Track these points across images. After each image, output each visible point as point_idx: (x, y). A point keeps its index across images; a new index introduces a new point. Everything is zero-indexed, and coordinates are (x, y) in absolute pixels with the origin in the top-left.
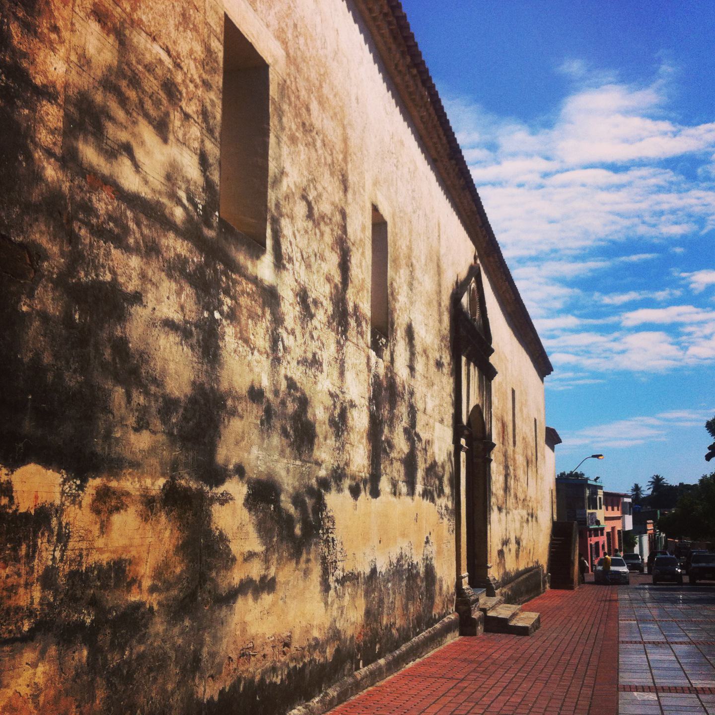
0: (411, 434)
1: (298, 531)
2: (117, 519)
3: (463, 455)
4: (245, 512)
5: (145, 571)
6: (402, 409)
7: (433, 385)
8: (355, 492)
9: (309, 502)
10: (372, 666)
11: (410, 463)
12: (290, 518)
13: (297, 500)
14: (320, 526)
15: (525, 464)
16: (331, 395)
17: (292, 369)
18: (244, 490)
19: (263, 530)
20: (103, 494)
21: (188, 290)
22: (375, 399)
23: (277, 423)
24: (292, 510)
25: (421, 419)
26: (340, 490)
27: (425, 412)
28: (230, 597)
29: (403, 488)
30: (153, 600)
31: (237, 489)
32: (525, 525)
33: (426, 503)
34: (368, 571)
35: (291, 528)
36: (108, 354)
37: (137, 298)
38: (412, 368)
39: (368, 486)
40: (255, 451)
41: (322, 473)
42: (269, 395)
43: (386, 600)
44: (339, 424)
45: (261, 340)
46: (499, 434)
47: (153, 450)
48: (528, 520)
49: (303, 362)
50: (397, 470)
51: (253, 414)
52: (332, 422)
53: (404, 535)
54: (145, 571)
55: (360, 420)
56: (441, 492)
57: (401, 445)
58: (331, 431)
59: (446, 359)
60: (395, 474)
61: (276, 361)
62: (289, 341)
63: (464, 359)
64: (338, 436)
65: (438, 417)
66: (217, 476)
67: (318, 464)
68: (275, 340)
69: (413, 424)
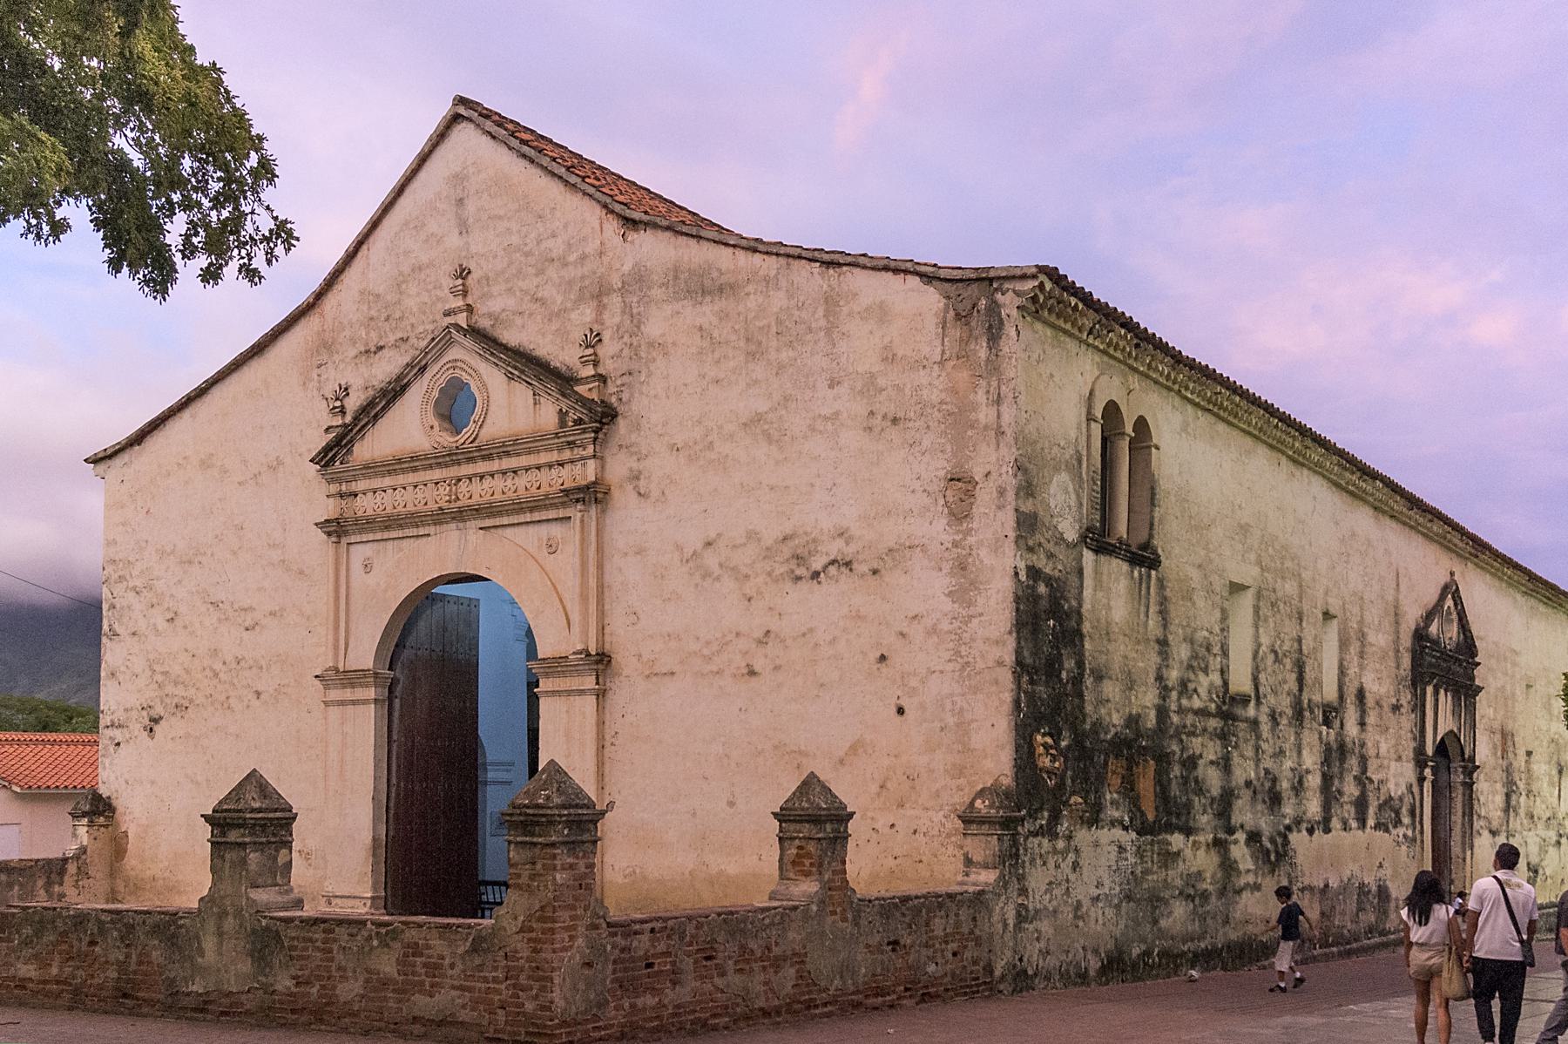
0: (1362, 780)
1: (1273, 858)
2: (1198, 853)
3: (1427, 786)
4: (1245, 850)
5: (1208, 875)
6: (1353, 762)
7: (1387, 729)
8: (1311, 831)
9: (1279, 840)
10: (1327, 950)
11: (1361, 805)
12: (1268, 851)
13: (1272, 840)
14: (1286, 854)
15: (1555, 772)
16: (1292, 770)
17: (1268, 763)
18: (1245, 836)
20: (1195, 842)
21: (1218, 742)
22: (1326, 761)
23: (1259, 797)
24: (1269, 845)
25: (1372, 765)
26: (1299, 831)
27: (1377, 756)
28: (1239, 892)
29: (1354, 824)
30: (1210, 888)
31: (1241, 836)
32: (1552, 850)
33: (1379, 834)
34: (1322, 885)
35: (1269, 857)
37: (1201, 756)
38: (1362, 724)
39: (1321, 826)
41: (1287, 821)
42: (1255, 782)
43: (1337, 907)
44: (1298, 787)
45: (1249, 752)
46: (1495, 747)
47: (1209, 822)
48: (1559, 843)
49: (1275, 755)
50: (1349, 811)
51: (1246, 794)
52: (1294, 788)
53: (1354, 860)
54: (1208, 875)
55: (1314, 781)
56: (1398, 822)
57: (1351, 789)
58: (1292, 794)
59: (1406, 698)
60: (1346, 815)
61: (1258, 761)
62: (1264, 746)
63: (1430, 689)
64: (1297, 795)
65: (1394, 756)
66: (1231, 831)
67: (1284, 817)
68: (1257, 748)
69: (1364, 770)
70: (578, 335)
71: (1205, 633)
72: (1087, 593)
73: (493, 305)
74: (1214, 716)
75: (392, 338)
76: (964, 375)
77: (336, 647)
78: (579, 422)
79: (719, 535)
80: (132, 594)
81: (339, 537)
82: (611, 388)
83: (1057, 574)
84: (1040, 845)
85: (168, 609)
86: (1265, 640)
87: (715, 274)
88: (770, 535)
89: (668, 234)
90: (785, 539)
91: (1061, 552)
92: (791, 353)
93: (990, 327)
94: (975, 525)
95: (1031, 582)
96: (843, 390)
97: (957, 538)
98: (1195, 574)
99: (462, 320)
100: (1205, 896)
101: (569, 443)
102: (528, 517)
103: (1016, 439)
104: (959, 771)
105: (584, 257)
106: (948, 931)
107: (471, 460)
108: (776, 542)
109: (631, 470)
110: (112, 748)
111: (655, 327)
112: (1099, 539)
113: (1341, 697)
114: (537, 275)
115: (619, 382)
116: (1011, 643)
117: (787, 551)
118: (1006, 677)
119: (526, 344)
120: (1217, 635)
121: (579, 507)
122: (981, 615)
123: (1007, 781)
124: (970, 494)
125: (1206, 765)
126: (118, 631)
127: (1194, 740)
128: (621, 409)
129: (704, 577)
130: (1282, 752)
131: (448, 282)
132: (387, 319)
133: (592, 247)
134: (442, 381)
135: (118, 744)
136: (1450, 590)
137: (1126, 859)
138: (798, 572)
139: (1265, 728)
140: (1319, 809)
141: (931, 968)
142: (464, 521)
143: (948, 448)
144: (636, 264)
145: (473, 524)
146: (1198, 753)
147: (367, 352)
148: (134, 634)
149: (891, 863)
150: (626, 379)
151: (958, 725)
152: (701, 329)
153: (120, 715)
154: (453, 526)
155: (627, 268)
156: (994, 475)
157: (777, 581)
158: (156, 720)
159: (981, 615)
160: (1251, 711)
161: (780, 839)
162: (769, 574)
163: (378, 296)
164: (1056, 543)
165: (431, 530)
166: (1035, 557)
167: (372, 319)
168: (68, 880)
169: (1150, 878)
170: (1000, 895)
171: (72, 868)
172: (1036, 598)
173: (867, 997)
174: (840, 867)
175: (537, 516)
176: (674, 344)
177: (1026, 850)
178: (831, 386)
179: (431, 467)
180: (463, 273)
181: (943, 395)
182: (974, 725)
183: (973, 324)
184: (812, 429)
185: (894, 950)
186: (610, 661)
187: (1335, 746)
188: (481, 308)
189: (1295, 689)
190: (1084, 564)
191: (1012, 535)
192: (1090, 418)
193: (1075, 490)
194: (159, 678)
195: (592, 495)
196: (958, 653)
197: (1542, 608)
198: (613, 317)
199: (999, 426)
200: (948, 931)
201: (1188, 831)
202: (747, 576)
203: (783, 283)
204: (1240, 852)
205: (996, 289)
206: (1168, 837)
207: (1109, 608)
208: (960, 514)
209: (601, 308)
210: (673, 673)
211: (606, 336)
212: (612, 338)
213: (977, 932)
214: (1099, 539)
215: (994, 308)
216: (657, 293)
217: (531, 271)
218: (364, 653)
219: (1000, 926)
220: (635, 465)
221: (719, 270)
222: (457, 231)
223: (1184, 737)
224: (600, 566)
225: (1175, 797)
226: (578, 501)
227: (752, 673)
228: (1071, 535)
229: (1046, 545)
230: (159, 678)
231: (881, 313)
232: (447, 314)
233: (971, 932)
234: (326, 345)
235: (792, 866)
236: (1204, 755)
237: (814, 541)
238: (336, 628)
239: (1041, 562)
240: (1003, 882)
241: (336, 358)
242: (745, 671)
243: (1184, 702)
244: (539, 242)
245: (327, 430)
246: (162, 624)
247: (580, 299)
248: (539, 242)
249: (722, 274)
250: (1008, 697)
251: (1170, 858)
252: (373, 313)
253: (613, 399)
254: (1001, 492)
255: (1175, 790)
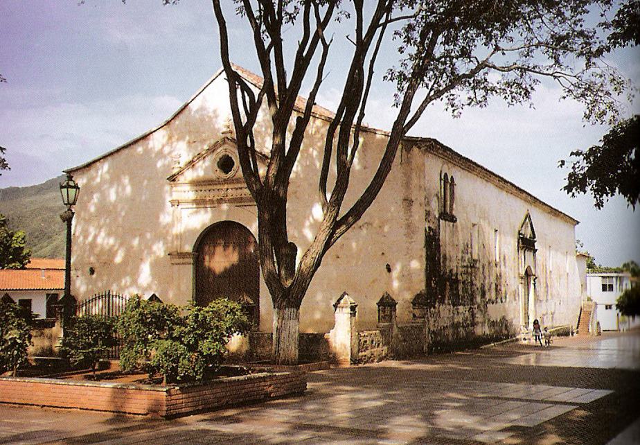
55: (493, 286)
97: (407, 218)
116: (425, 250)
134: (221, 155)
136: (528, 217)
192: (441, 179)
196: (407, 252)
197: (553, 218)
228: (437, 216)
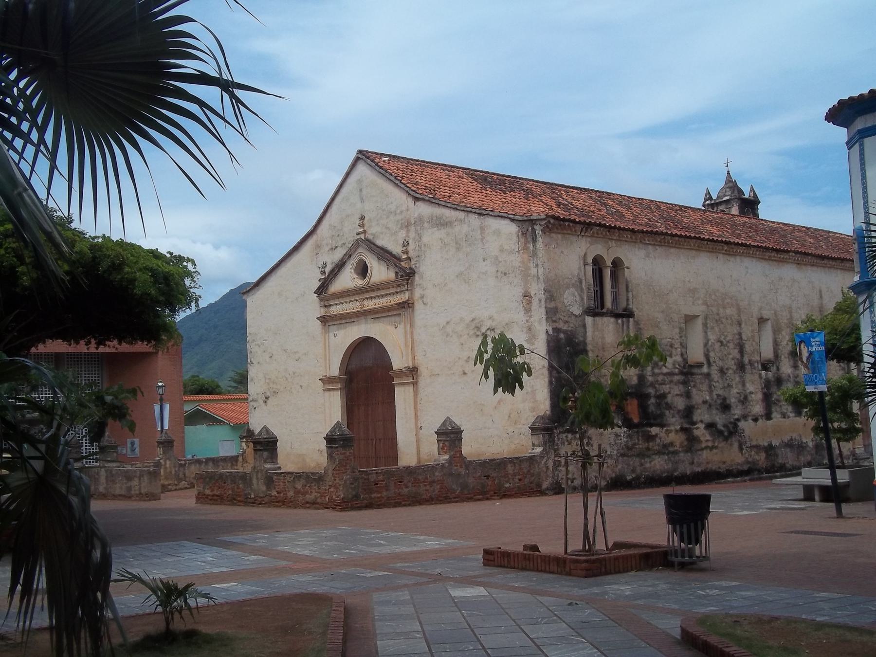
2: (670, 435)
5: (678, 444)
13: (725, 426)
16: (738, 393)
18: (704, 426)
19: (711, 434)
20: (667, 430)
30: (681, 450)
36: (664, 406)
40: (706, 416)
41: (736, 417)
47: (676, 421)
54: (678, 444)
70: (401, 242)
71: (670, 340)
72: (589, 334)
73: (373, 230)
74: (677, 375)
75: (340, 243)
76: (526, 256)
77: (326, 367)
78: (402, 276)
79: (451, 319)
80: (257, 347)
81: (325, 323)
82: (413, 263)
83: (570, 329)
84: (567, 437)
85: (270, 353)
86: (712, 337)
87: (444, 218)
88: (468, 319)
89: (428, 203)
90: (472, 320)
91: (573, 320)
92: (471, 248)
93: (533, 238)
94: (532, 314)
95: (555, 334)
96: (488, 262)
98: (660, 316)
99: (362, 236)
100: (675, 453)
101: (399, 284)
102: (387, 314)
103: (544, 280)
104: (533, 410)
105: (401, 212)
106: (515, 471)
107: (367, 292)
108: (470, 322)
109: (421, 294)
110: (253, 410)
111: (426, 239)
112: (597, 310)
113: (777, 356)
114: (387, 218)
115: (415, 260)
117: (473, 325)
118: (546, 372)
119: (384, 245)
120: (677, 339)
121: (403, 310)
122: (537, 348)
123: (548, 413)
124: (530, 302)
125: (673, 396)
126: (254, 362)
127: (664, 386)
128: (416, 270)
129: (447, 336)
130: (730, 386)
131: (358, 222)
132: (338, 236)
133: (404, 208)
135: (255, 408)
137: (621, 440)
138: (478, 333)
139: (715, 375)
140: (762, 410)
141: (507, 485)
142: (366, 315)
143: (522, 284)
144: (419, 214)
145: (369, 317)
146: (667, 391)
147: (332, 249)
148: (259, 363)
149: (513, 446)
150: (417, 259)
151: (532, 391)
152: (441, 239)
153: (255, 396)
154: (363, 318)
155: (416, 215)
156: (537, 295)
157: (470, 337)
158: (267, 398)
159: (537, 348)
160: (705, 369)
161: (438, 441)
162: (468, 334)
163: (335, 227)
164: (569, 317)
165: (355, 319)
166: (557, 324)
167: (333, 236)
168: (239, 464)
169: (637, 447)
170: (544, 457)
171: (240, 459)
172: (558, 340)
173: (475, 495)
174: (459, 449)
175: (390, 314)
176: (432, 245)
177: (558, 439)
178: (484, 261)
179: (354, 295)
180: (362, 218)
181: (520, 264)
182: (537, 391)
183: (528, 236)
184: (479, 277)
185: (487, 479)
186: (417, 370)
187: (773, 379)
188: (369, 231)
189: (738, 356)
190: (586, 322)
191: (544, 317)
192: (585, 264)
193: (579, 294)
194: (268, 381)
195: (406, 306)
198: (412, 234)
199: (538, 275)
200: (515, 471)
201: (662, 426)
202: (461, 336)
203: (466, 221)
204: (700, 431)
205: (534, 224)
206: (649, 429)
207: (603, 338)
208: (528, 310)
209: (408, 231)
210: (438, 374)
211: (410, 242)
212: (412, 243)
213: (532, 471)
214: (597, 310)
215: (534, 230)
216: (426, 225)
217: (385, 216)
218: (335, 371)
219: (544, 469)
220: (422, 293)
221: (446, 216)
222: (359, 202)
223: (657, 386)
224: (412, 333)
225: (652, 412)
226: (402, 308)
227: (465, 373)
229: (562, 318)
230: (268, 381)
231: (498, 233)
232: (358, 234)
233: (529, 471)
234: (318, 247)
235: (441, 450)
236: (672, 392)
237: (482, 321)
238: (326, 360)
239: (561, 325)
240: (545, 452)
241: (322, 251)
242: (462, 373)
243: (656, 371)
244: (387, 205)
245: (319, 280)
246: (268, 360)
247: (401, 228)
248: (387, 205)
249: (447, 218)
250: (547, 380)
251: (650, 438)
252: (334, 233)
253: (414, 267)
254: (540, 301)
255: (652, 408)
